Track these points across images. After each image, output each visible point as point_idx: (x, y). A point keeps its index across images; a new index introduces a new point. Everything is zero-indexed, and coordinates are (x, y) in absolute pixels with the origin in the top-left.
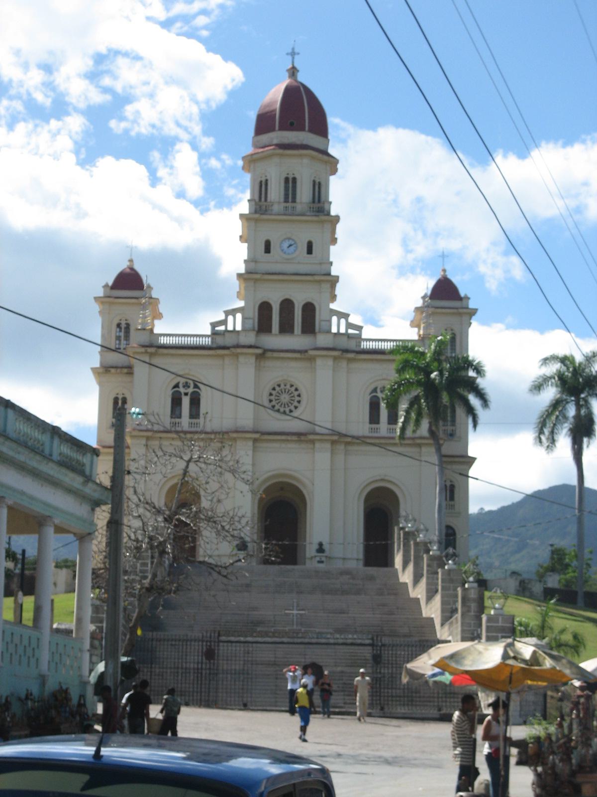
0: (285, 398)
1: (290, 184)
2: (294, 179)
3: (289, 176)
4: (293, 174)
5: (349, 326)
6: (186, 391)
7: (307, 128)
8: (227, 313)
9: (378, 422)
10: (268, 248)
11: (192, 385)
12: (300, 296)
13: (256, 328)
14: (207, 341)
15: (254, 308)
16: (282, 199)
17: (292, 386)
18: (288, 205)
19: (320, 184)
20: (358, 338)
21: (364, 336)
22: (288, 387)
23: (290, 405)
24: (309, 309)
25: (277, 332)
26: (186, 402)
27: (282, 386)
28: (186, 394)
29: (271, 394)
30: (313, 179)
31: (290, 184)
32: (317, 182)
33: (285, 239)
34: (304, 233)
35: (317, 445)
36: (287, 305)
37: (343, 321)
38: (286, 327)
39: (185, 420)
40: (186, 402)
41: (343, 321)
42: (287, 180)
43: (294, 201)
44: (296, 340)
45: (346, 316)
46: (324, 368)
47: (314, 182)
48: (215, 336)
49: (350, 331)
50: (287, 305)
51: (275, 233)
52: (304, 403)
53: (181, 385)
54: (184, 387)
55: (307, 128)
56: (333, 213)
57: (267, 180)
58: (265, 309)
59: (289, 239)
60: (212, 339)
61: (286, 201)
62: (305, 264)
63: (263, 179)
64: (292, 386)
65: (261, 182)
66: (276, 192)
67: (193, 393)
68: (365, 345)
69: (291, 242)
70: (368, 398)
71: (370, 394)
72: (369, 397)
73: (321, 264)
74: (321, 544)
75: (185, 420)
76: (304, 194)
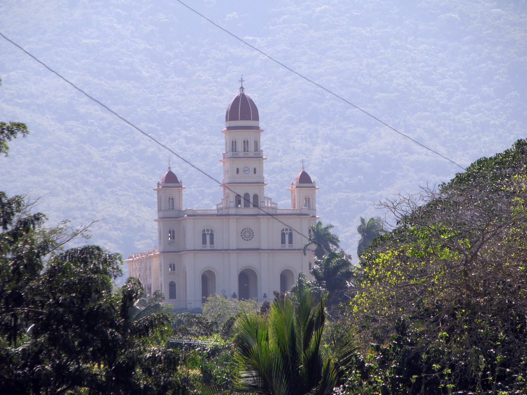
1: (246, 143)
2: (247, 141)
5: (272, 203)
9: (285, 243)
11: (210, 230)
12: (252, 191)
17: (250, 229)
22: (248, 230)
24: (256, 197)
26: (208, 237)
31: (246, 143)
34: (252, 164)
36: (247, 195)
37: (269, 201)
38: (247, 205)
39: (208, 246)
40: (208, 237)
41: (269, 201)
42: (244, 141)
44: (252, 210)
45: (271, 199)
46: (264, 221)
49: (273, 206)
50: (247, 195)
51: (241, 164)
53: (206, 230)
57: (235, 141)
58: (238, 196)
60: (218, 211)
61: (245, 151)
62: (253, 178)
63: (234, 141)
65: (233, 142)
66: (240, 147)
74: (265, 294)
75: (208, 246)
76: (252, 147)
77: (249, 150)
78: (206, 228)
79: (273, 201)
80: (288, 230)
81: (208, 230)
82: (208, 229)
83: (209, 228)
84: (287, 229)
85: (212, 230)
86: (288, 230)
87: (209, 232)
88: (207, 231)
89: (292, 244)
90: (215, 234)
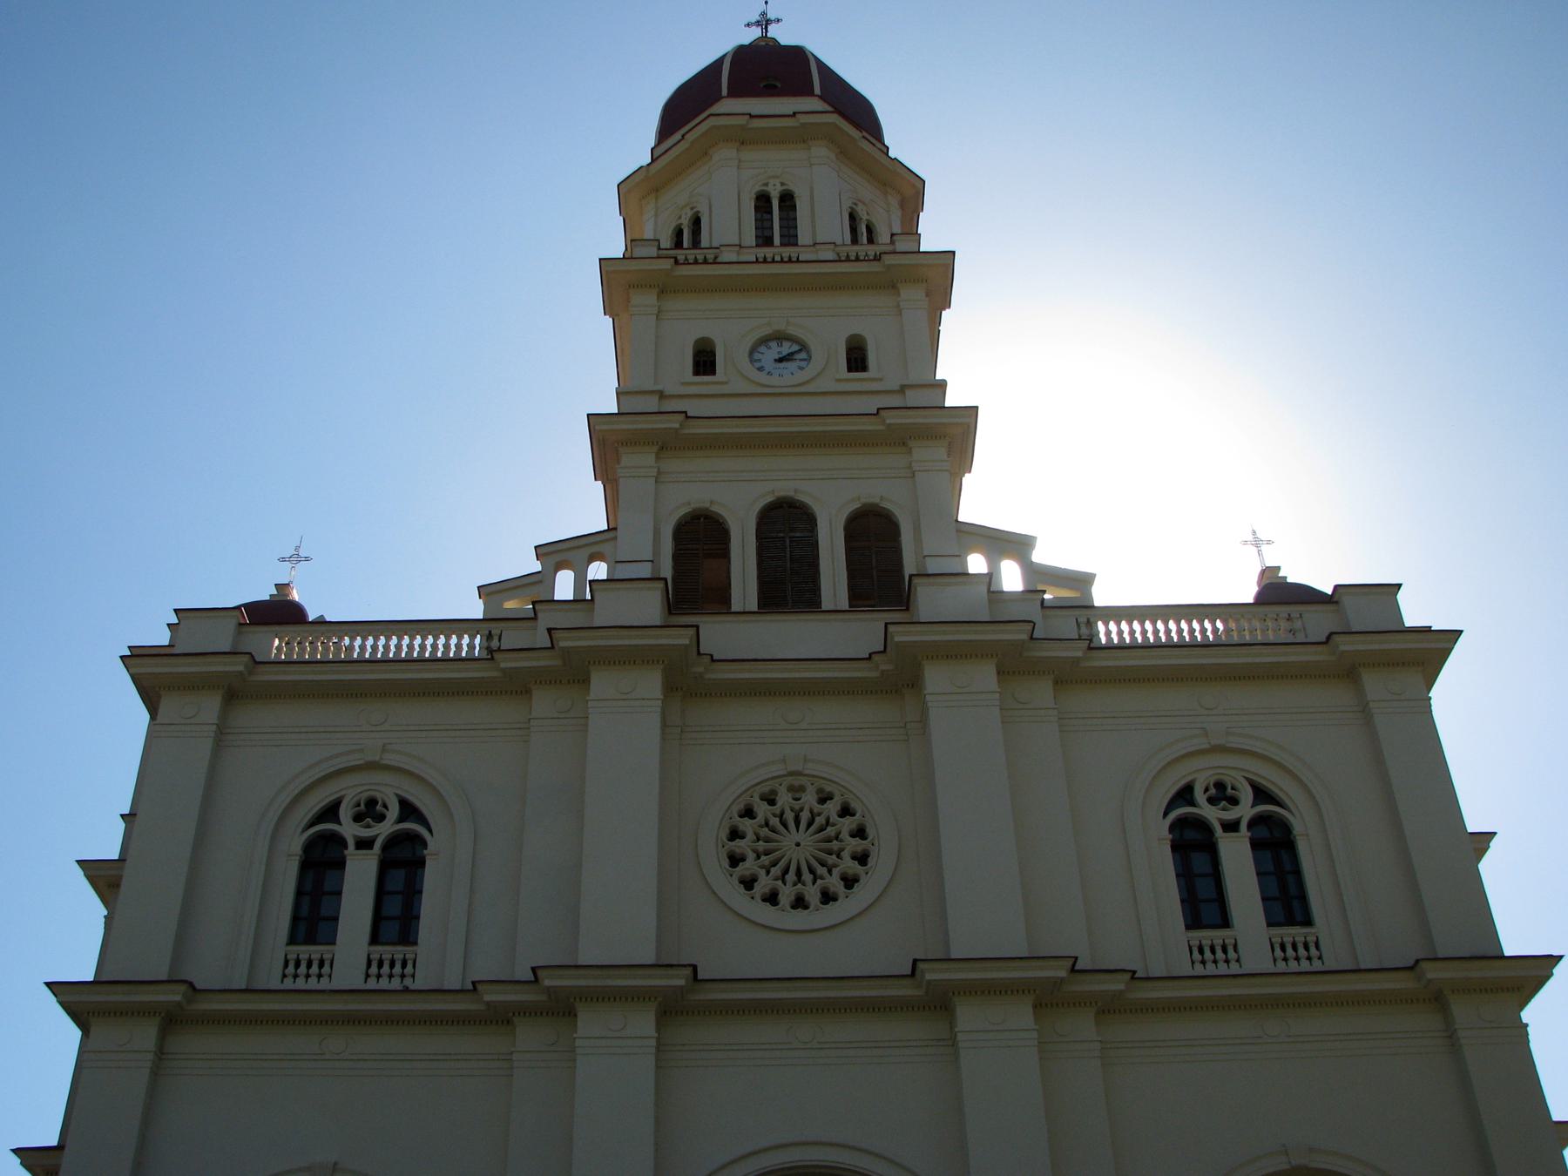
0: (798, 846)
2: (787, 199)
3: (770, 189)
4: (782, 184)
6: (366, 833)
7: (817, 91)
8: (555, 554)
10: (704, 361)
11: (394, 811)
13: (667, 571)
14: (468, 645)
15: (657, 532)
16: (750, 237)
17: (824, 798)
18: (768, 252)
19: (870, 230)
20: (1084, 612)
21: (1099, 601)
22: (810, 799)
23: (821, 870)
25: (753, 605)
27: (784, 799)
28: (364, 844)
29: (735, 834)
30: (847, 204)
32: (862, 212)
33: (764, 341)
35: (969, 1016)
42: (763, 201)
43: (790, 238)
47: (853, 217)
48: (496, 628)
52: (882, 862)
53: (345, 813)
54: (358, 818)
55: (817, 91)
56: (932, 236)
57: (696, 222)
59: (780, 337)
60: (490, 636)
61: (765, 240)
64: (824, 798)
65: (679, 233)
67: (393, 841)
68: (1106, 632)
69: (787, 348)
70: (1161, 830)
71: (1166, 814)
72: (1165, 832)
73: (903, 389)
77: (804, 236)
78: (352, 791)
79: (1039, 556)
80: (1234, 801)
81: (370, 811)
82: (372, 802)
83: (388, 790)
84: (1220, 786)
85: (408, 810)
86: (1234, 801)
87: (384, 830)
88: (358, 818)
89: (1308, 922)
90: (436, 844)
